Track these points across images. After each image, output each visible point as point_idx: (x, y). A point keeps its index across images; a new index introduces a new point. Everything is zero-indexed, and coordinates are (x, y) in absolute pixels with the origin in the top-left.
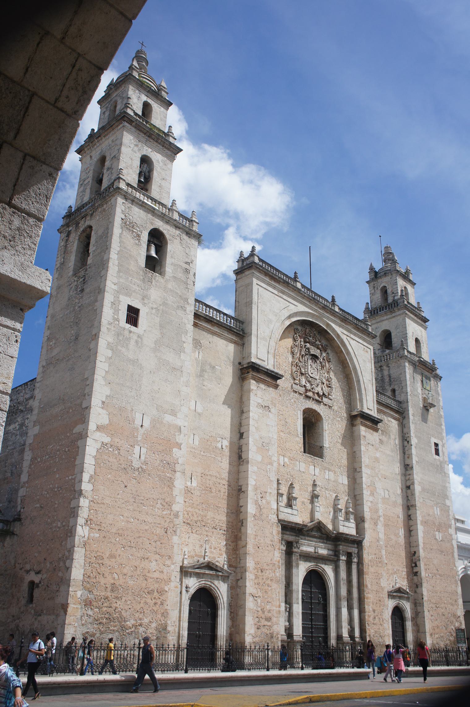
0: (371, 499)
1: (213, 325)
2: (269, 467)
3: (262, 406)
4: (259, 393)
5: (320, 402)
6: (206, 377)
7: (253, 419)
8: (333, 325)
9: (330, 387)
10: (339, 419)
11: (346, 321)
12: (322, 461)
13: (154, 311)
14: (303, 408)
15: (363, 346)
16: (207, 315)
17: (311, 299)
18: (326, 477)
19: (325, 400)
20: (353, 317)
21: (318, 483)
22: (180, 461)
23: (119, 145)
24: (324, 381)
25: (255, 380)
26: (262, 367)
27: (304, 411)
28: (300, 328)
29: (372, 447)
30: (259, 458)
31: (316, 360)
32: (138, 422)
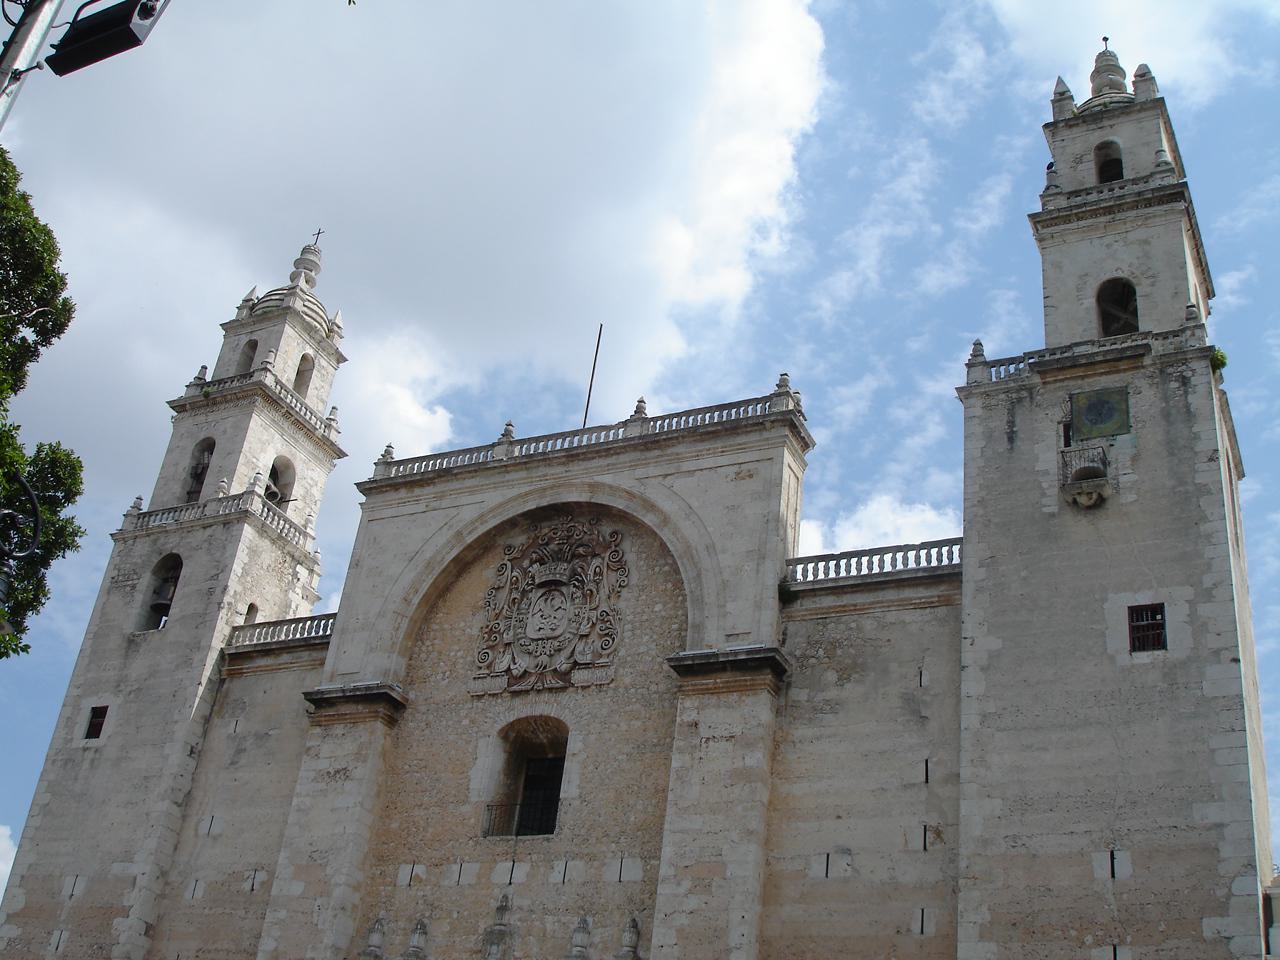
0: (693, 903)
1: (278, 655)
2: (319, 901)
3: (329, 773)
4: (326, 749)
5: (563, 689)
6: (243, 761)
7: (299, 810)
8: (607, 479)
9: (607, 635)
10: (638, 706)
11: (658, 441)
12: (548, 840)
13: (132, 696)
14: (498, 727)
15: (735, 469)
16: (256, 645)
17: (525, 463)
18: (551, 880)
19: (579, 676)
20: (710, 409)
21: (516, 902)
22: (122, 939)
23: (241, 431)
24: (584, 630)
25: (320, 726)
26: (330, 692)
27: (505, 734)
28: (519, 540)
29: (723, 744)
30: (297, 888)
31: (564, 589)
32: (66, 892)
